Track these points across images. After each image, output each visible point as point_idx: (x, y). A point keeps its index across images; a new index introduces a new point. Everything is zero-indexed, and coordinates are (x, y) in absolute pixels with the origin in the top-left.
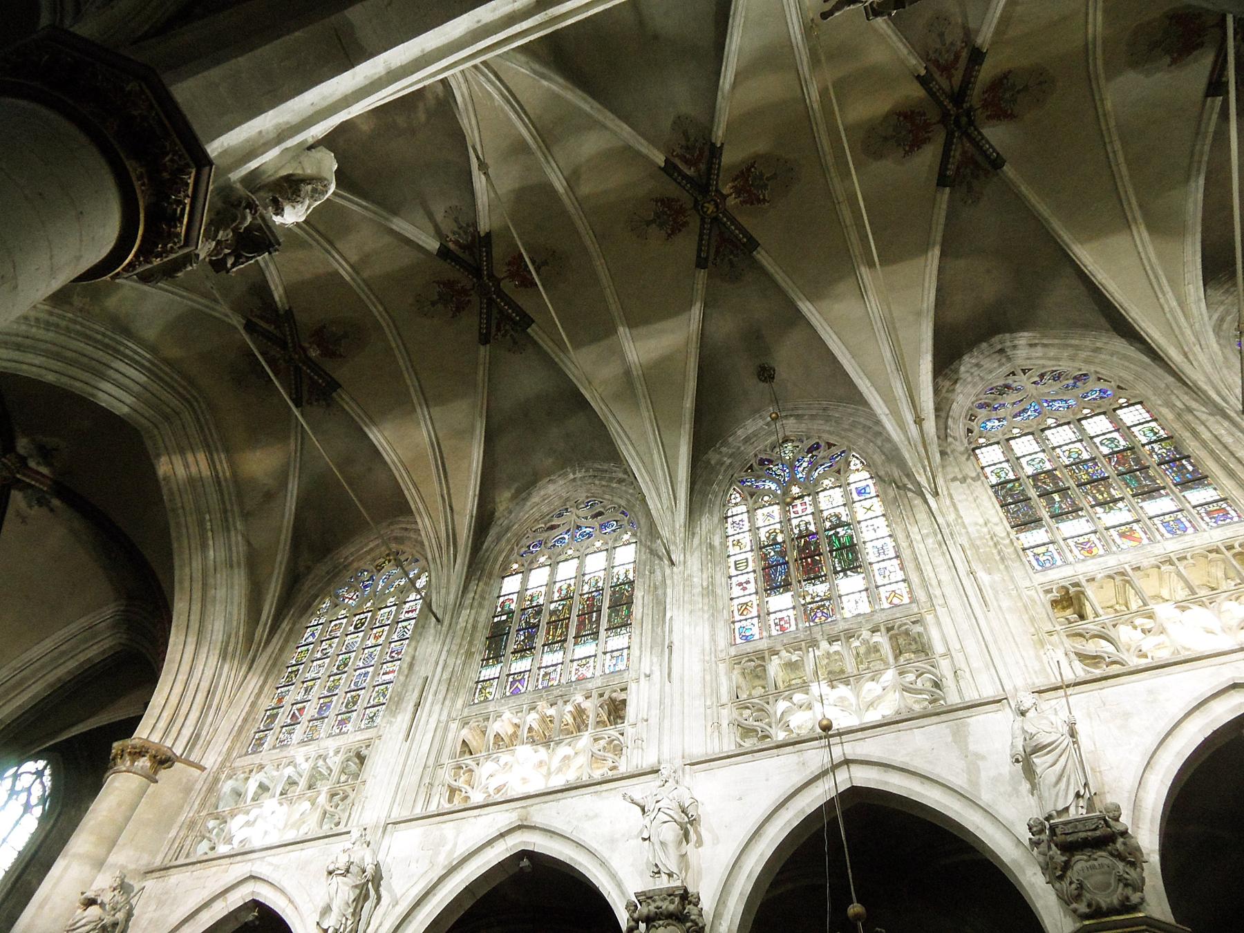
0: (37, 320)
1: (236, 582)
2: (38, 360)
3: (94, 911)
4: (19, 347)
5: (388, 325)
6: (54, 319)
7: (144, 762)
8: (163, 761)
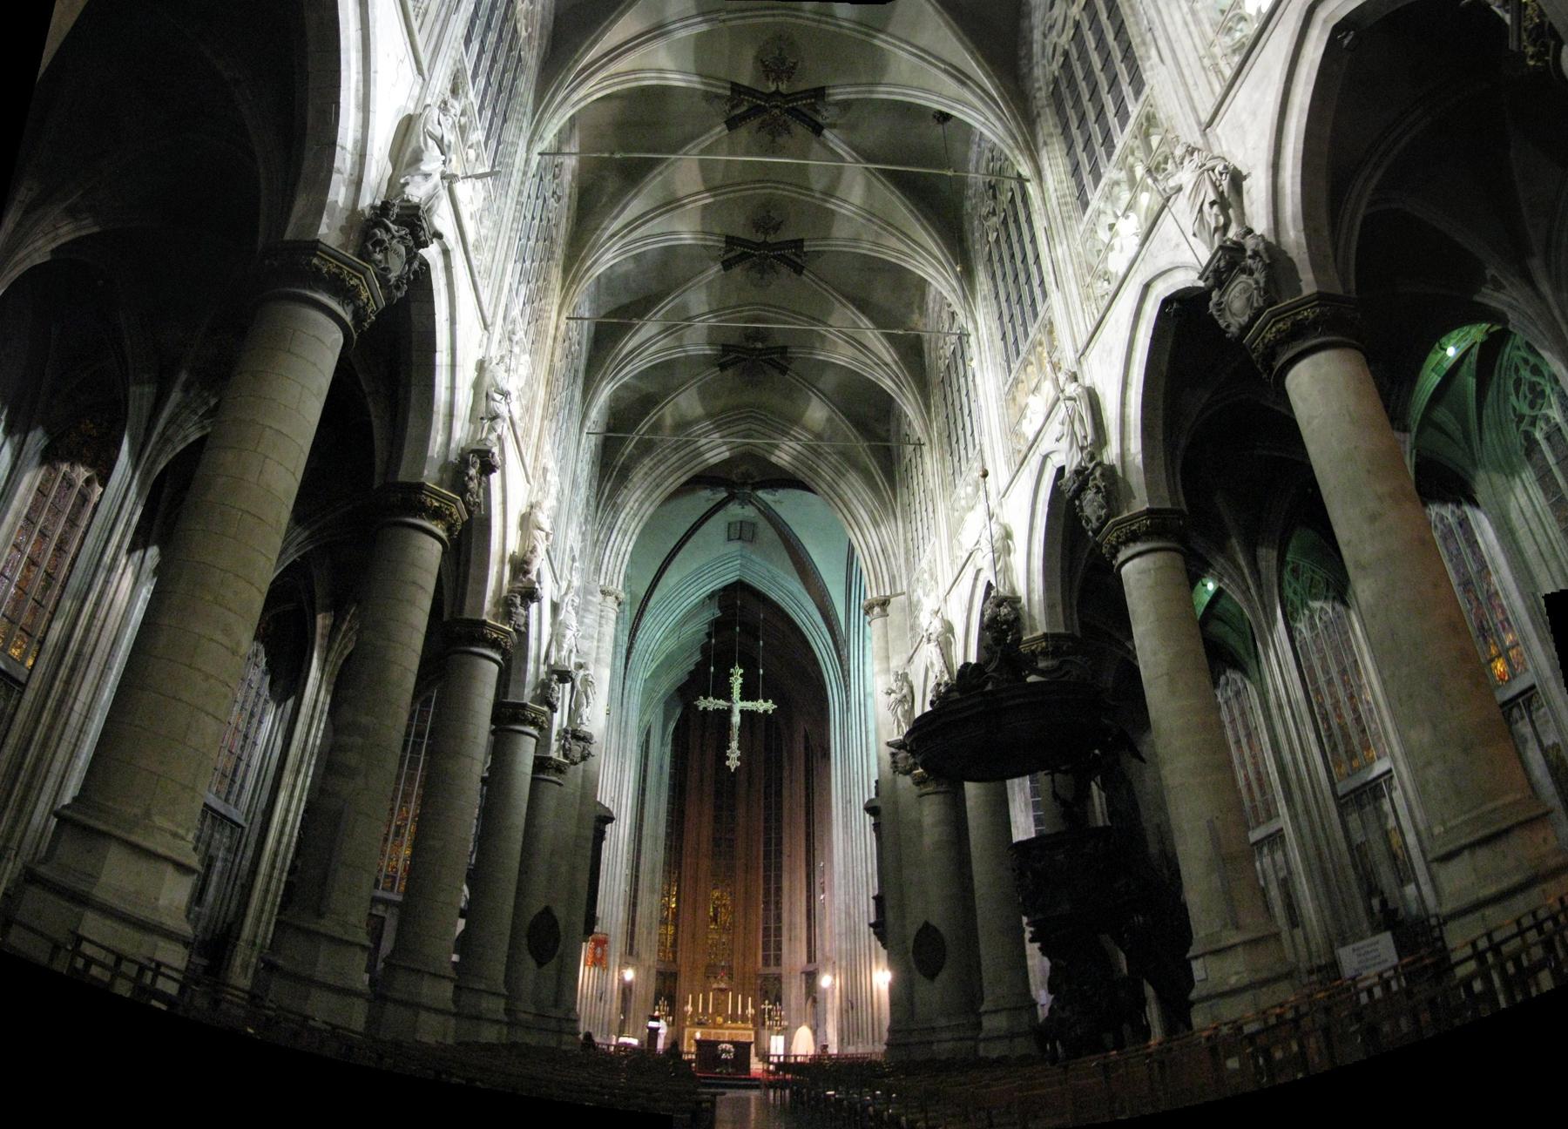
0: (650, 468)
1: (853, 481)
2: (671, 480)
3: (893, 695)
4: (658, 486)
7: (877, 610)
8: (884, 603)
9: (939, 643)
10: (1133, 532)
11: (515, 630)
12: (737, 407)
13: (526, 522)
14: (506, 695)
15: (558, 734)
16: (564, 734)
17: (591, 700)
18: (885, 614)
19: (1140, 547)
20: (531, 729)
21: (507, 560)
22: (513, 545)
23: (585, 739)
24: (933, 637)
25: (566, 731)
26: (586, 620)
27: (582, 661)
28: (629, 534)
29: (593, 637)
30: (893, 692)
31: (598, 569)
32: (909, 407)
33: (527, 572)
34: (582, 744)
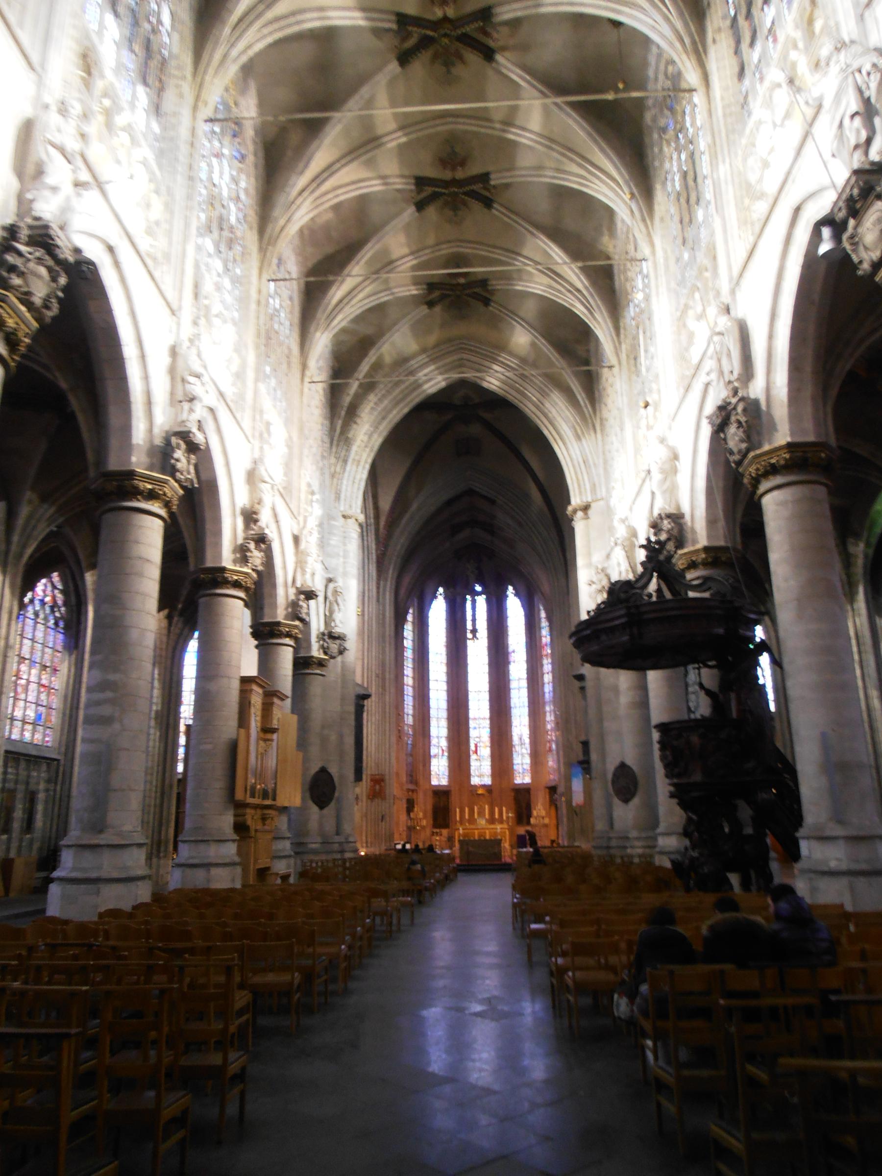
1: (557, 400)
2: (395, 412)
3: (594, 586)
4: (384, 418)
5: (458, 246)
6: (379, 395)
7: (580, 514)
8: (586, 508)
9: (624, 547)
10: (773, 466)
11: (253, 570)
12: (450, 340)
13: (252, 477)
14: (262, 617)
15: (318, 637)
16: (322, 636)
17: (342, 607)
18: (587, 517)
19: (778, 480)
20: (287, 641)
21: (238, 511)
22: (243, 499)
23: (340, 638)
24: (619, 542)
25: (323, 634)
26: (332, 542)
27: (331, 576)
28: (362, 463)
29: (339, 555)
30: (594, 583)
31: (338, 498)
32: (601, 328)
33: (256, 521)
34: (338, 642)
